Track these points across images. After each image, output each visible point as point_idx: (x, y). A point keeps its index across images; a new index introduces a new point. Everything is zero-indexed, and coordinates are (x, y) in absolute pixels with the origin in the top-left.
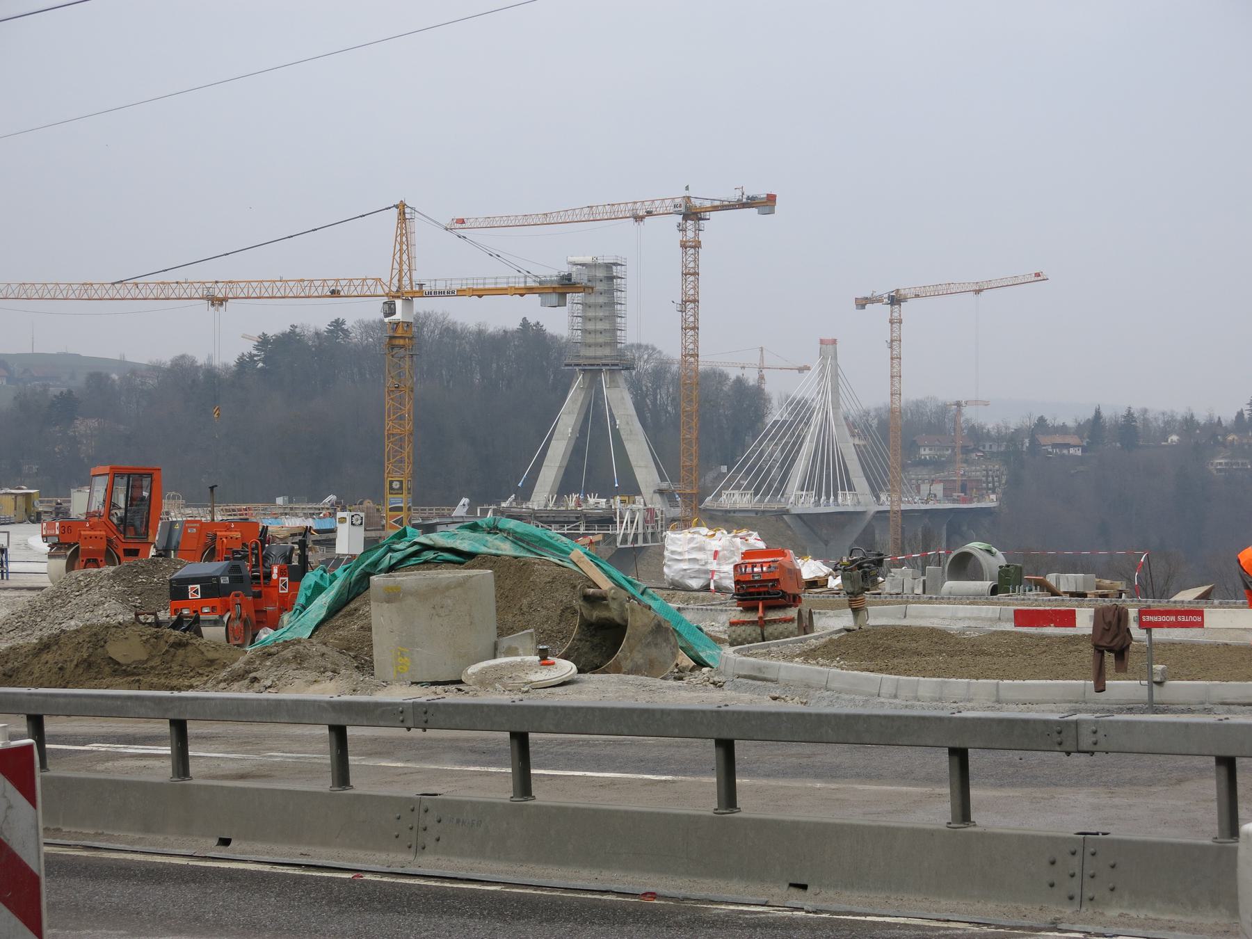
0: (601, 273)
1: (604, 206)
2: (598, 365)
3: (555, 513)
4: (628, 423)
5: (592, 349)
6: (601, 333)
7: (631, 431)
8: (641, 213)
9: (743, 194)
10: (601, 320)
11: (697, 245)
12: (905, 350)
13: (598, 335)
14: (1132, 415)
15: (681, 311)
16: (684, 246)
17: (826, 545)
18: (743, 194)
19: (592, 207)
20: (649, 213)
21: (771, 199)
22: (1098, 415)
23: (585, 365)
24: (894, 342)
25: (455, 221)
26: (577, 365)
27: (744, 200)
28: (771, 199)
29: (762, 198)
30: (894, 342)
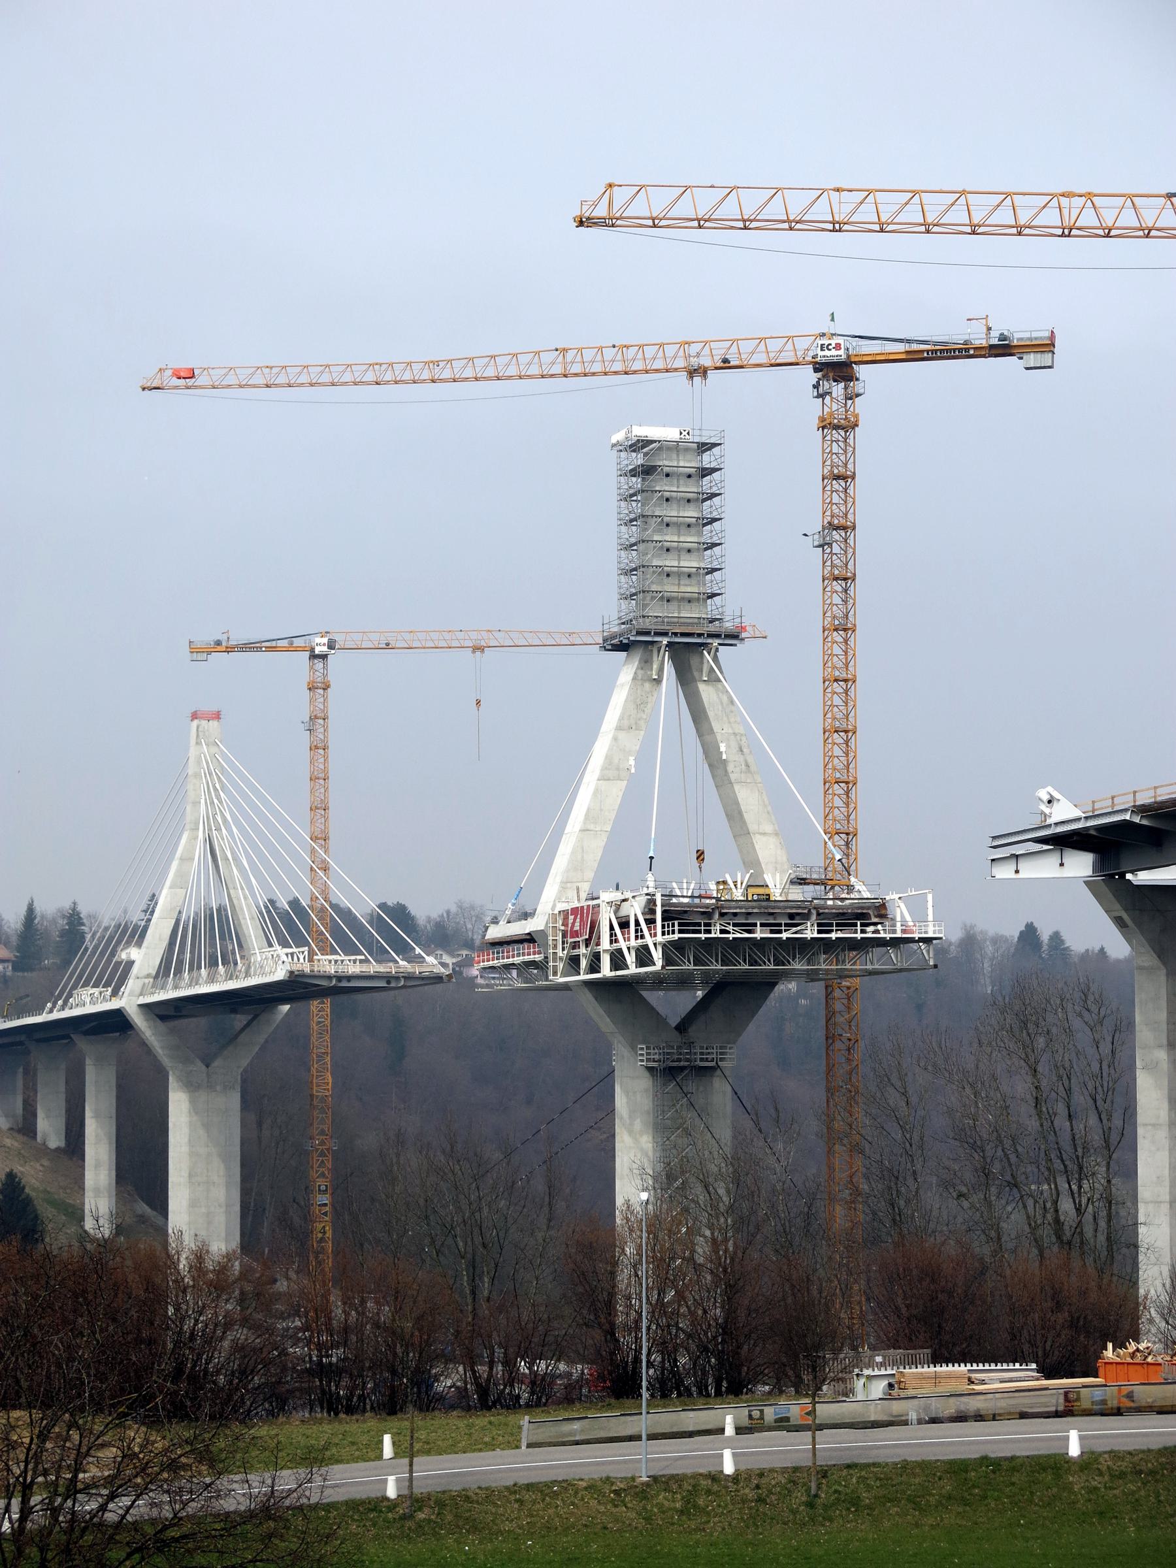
0: (688, 463)
1: (601, 348)
2: (700, 635)
3: (759, 908)
4: (741, 751)
5: (673, 605)
6: (689, 576)
7: (747, 766)
8: (707, 362)
9: (989, 329)
10: (689, 551)
11: (848, 426)
12: (337, 733)
13: (685, 581)
14: (78, 914)
15: (821, 546)
16: (826, 425)
17: (207, 1066)
18: (989, 329)
19: (565, 350)
20: (726, 364)
21: (1047, 346)
22: (31, 910)
23: (675, 634)
24: (317, 720)
25: (169, 373)
26: (665, 634)
27: (995, 342)
28: (1047, 346)
29: (1041, 338)
30: (317, 720)
